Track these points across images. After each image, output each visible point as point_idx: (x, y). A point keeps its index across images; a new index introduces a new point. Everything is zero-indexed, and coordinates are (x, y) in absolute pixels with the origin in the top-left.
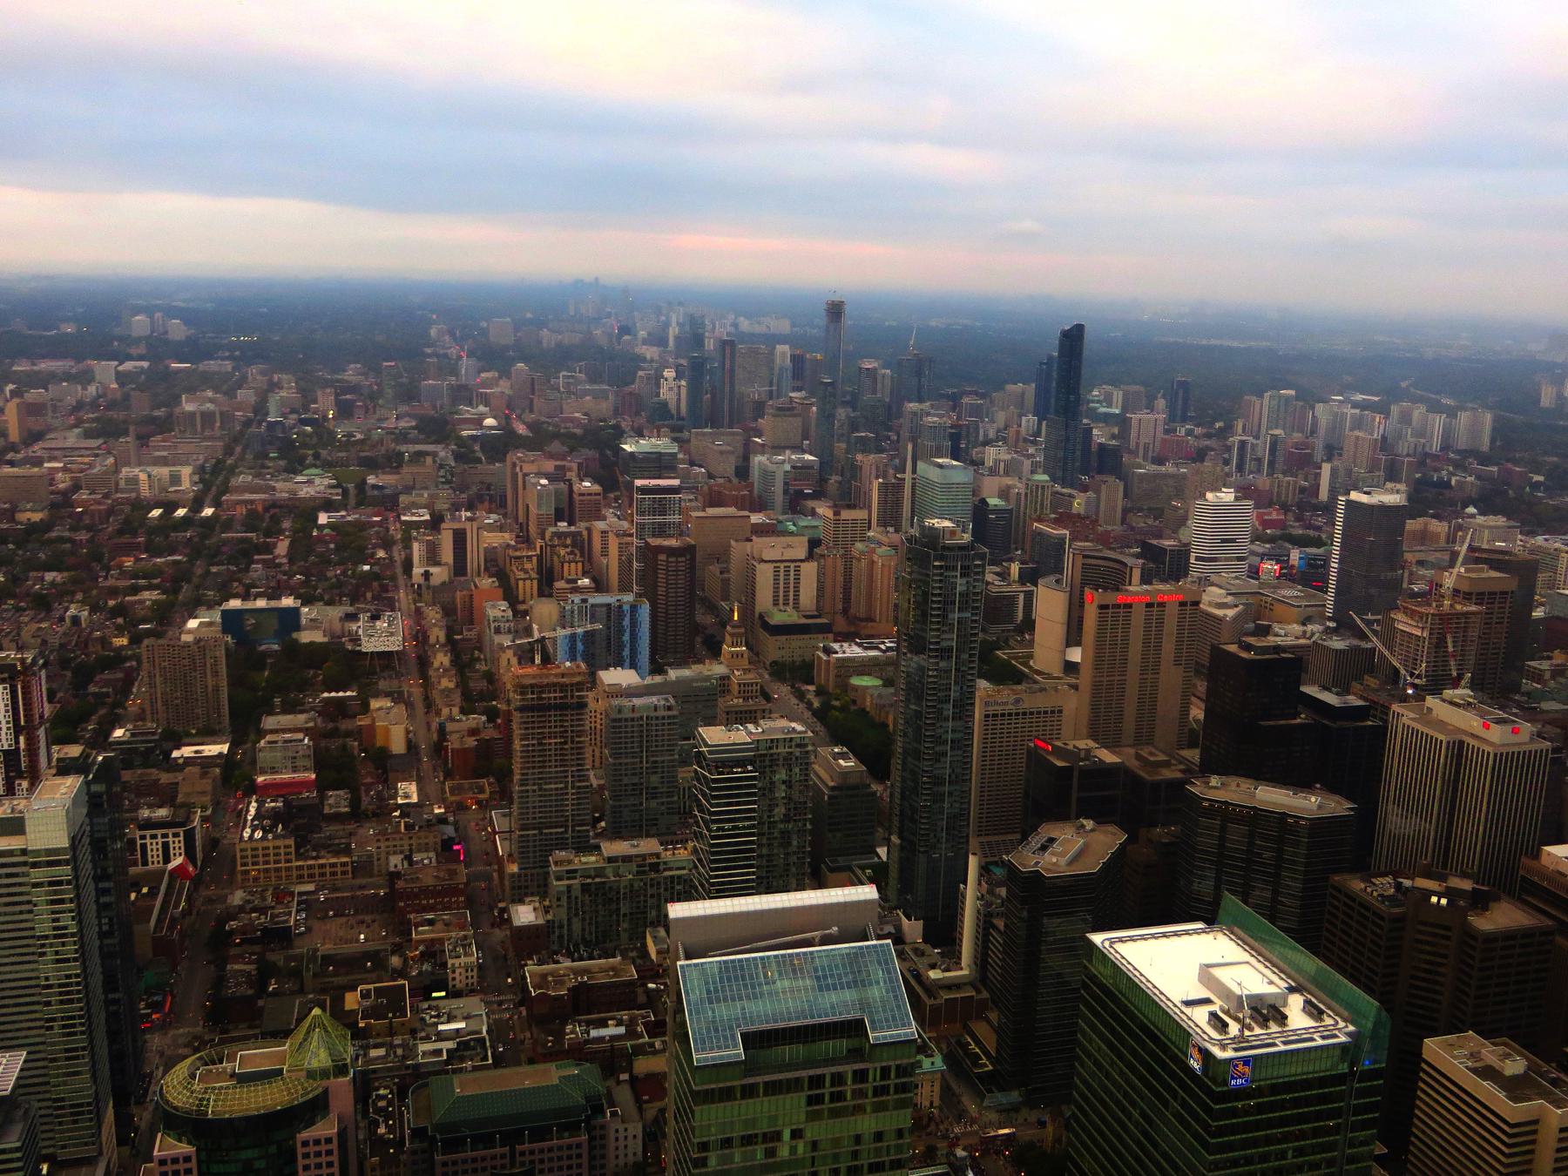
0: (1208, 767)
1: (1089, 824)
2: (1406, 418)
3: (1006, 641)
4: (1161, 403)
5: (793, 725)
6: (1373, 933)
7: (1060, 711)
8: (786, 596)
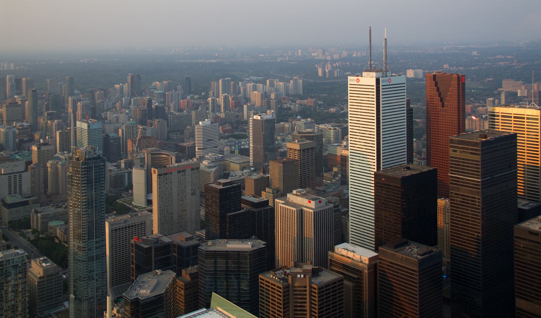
0: (210, 236)
1: (159, 271)
3: (121, 195)
4: (179, 87)
5: (18, 251)
6: (277, 294)
7: (145, 223)
8: (15, 189)
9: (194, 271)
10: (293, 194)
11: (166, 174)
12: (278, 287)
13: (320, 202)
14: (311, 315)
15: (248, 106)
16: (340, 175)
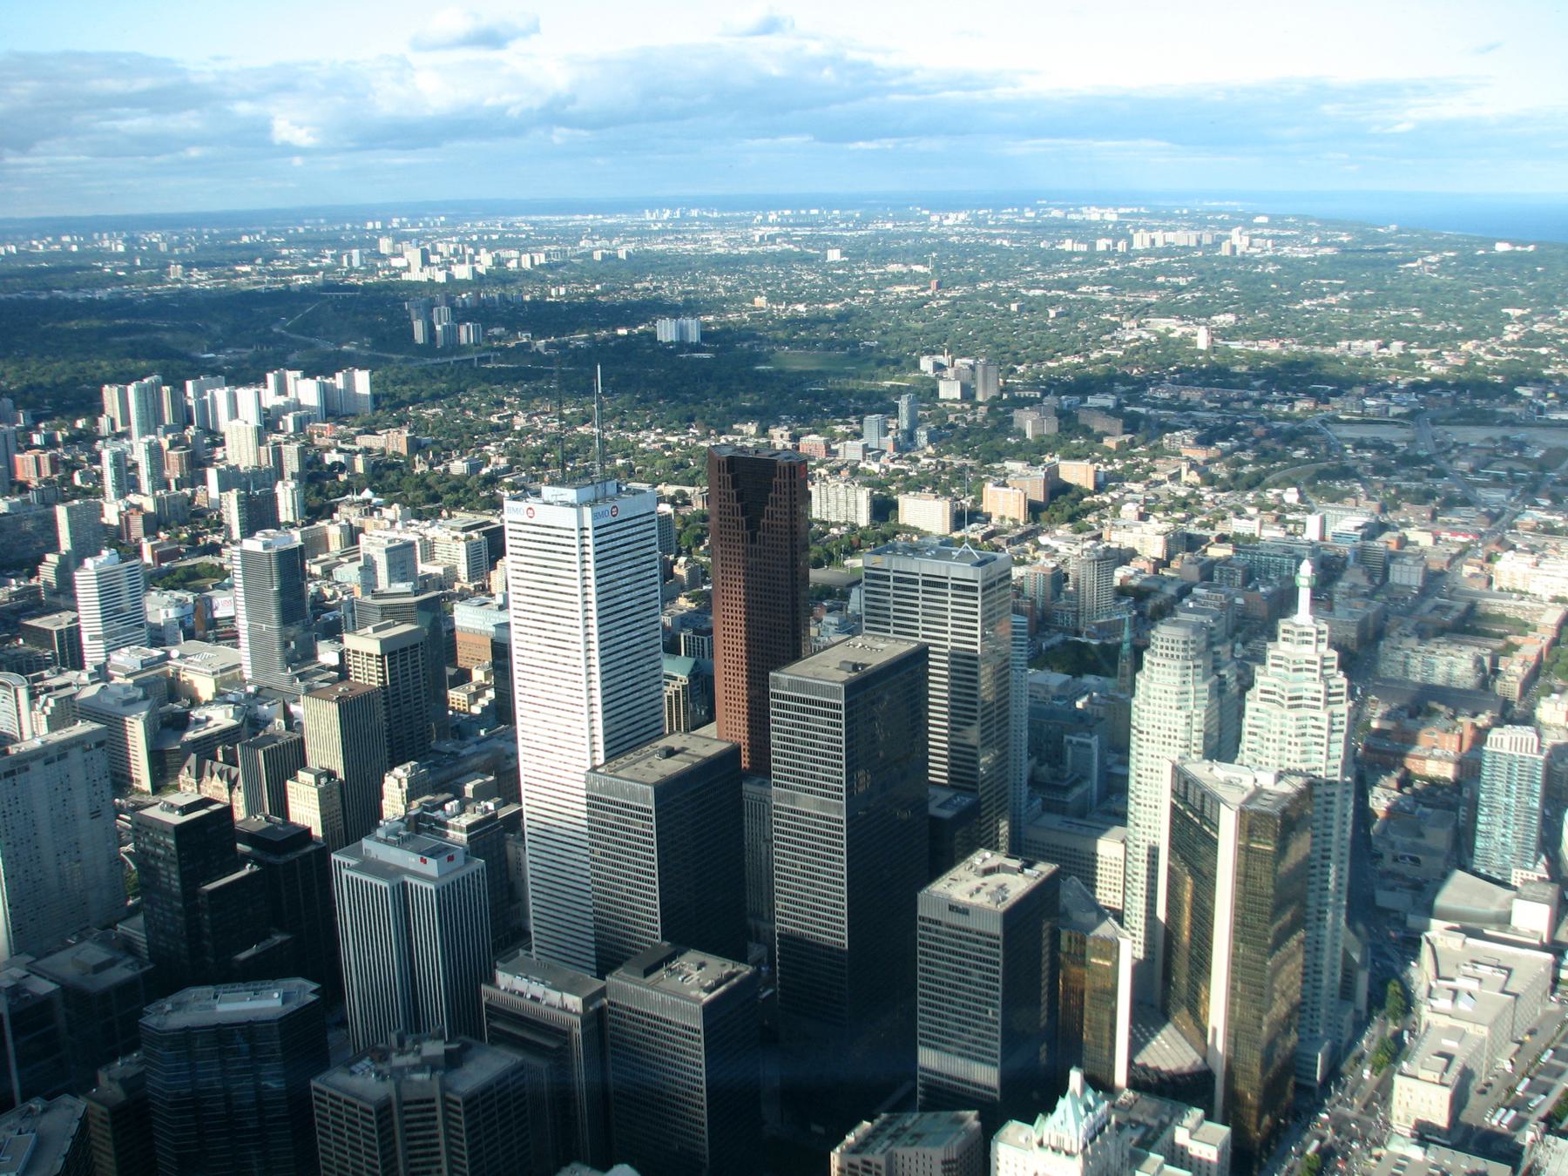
2: (282, 389)
9: (133, 1070)
10: (378, 840)
11: (12, 773)
12: (362, 1109)
13: (451, 859)
14: (451, 1171)
15: (219, 471)
16: (491, 694)
